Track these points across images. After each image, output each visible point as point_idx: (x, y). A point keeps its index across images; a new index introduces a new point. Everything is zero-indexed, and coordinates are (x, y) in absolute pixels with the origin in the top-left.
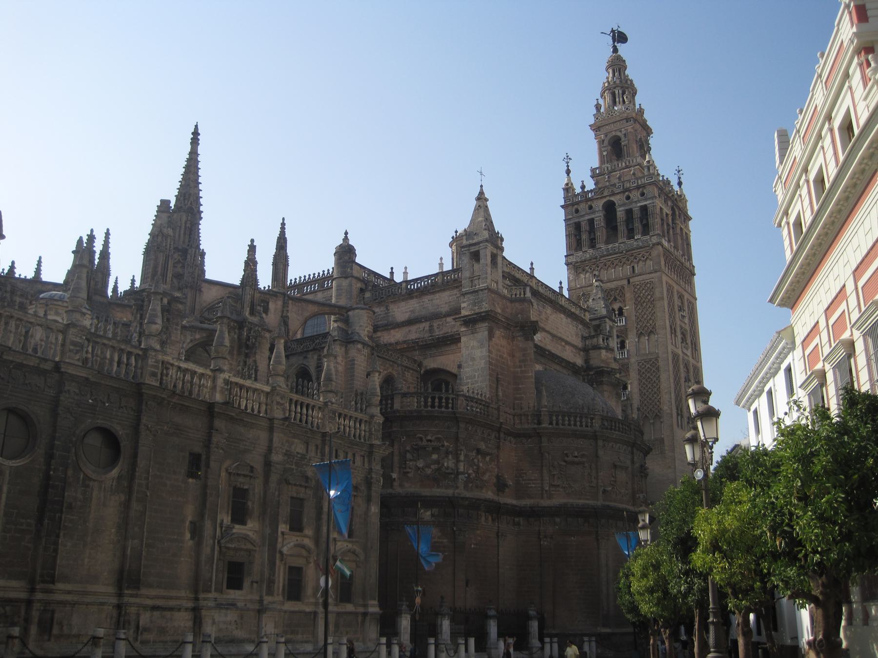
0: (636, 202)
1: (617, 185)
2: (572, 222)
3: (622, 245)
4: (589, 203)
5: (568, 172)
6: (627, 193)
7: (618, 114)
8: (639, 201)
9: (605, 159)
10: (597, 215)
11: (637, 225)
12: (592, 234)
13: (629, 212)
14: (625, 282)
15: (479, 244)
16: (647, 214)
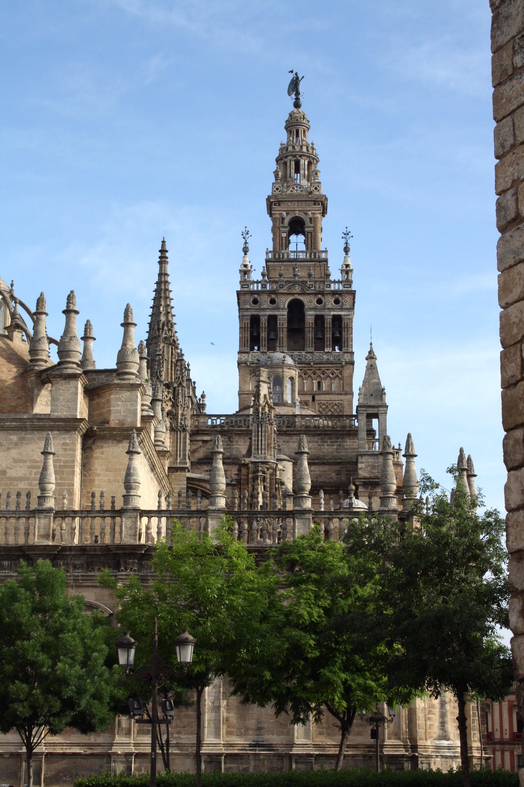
0: (329, 309)
1: (309, 283)
2: (249, 313)
3: (308, 355)
4: (273, 296)
5: (246, 251)
6: (320, 296)
7: (304, 193)
8: (333, 309)
9: (284, 242)
10: (281, 313)
11: (328, 335)
12: (272, 333)
13: (319, 319)
14: (310, 398)
15: (378, 408)
16: (340, 326)
